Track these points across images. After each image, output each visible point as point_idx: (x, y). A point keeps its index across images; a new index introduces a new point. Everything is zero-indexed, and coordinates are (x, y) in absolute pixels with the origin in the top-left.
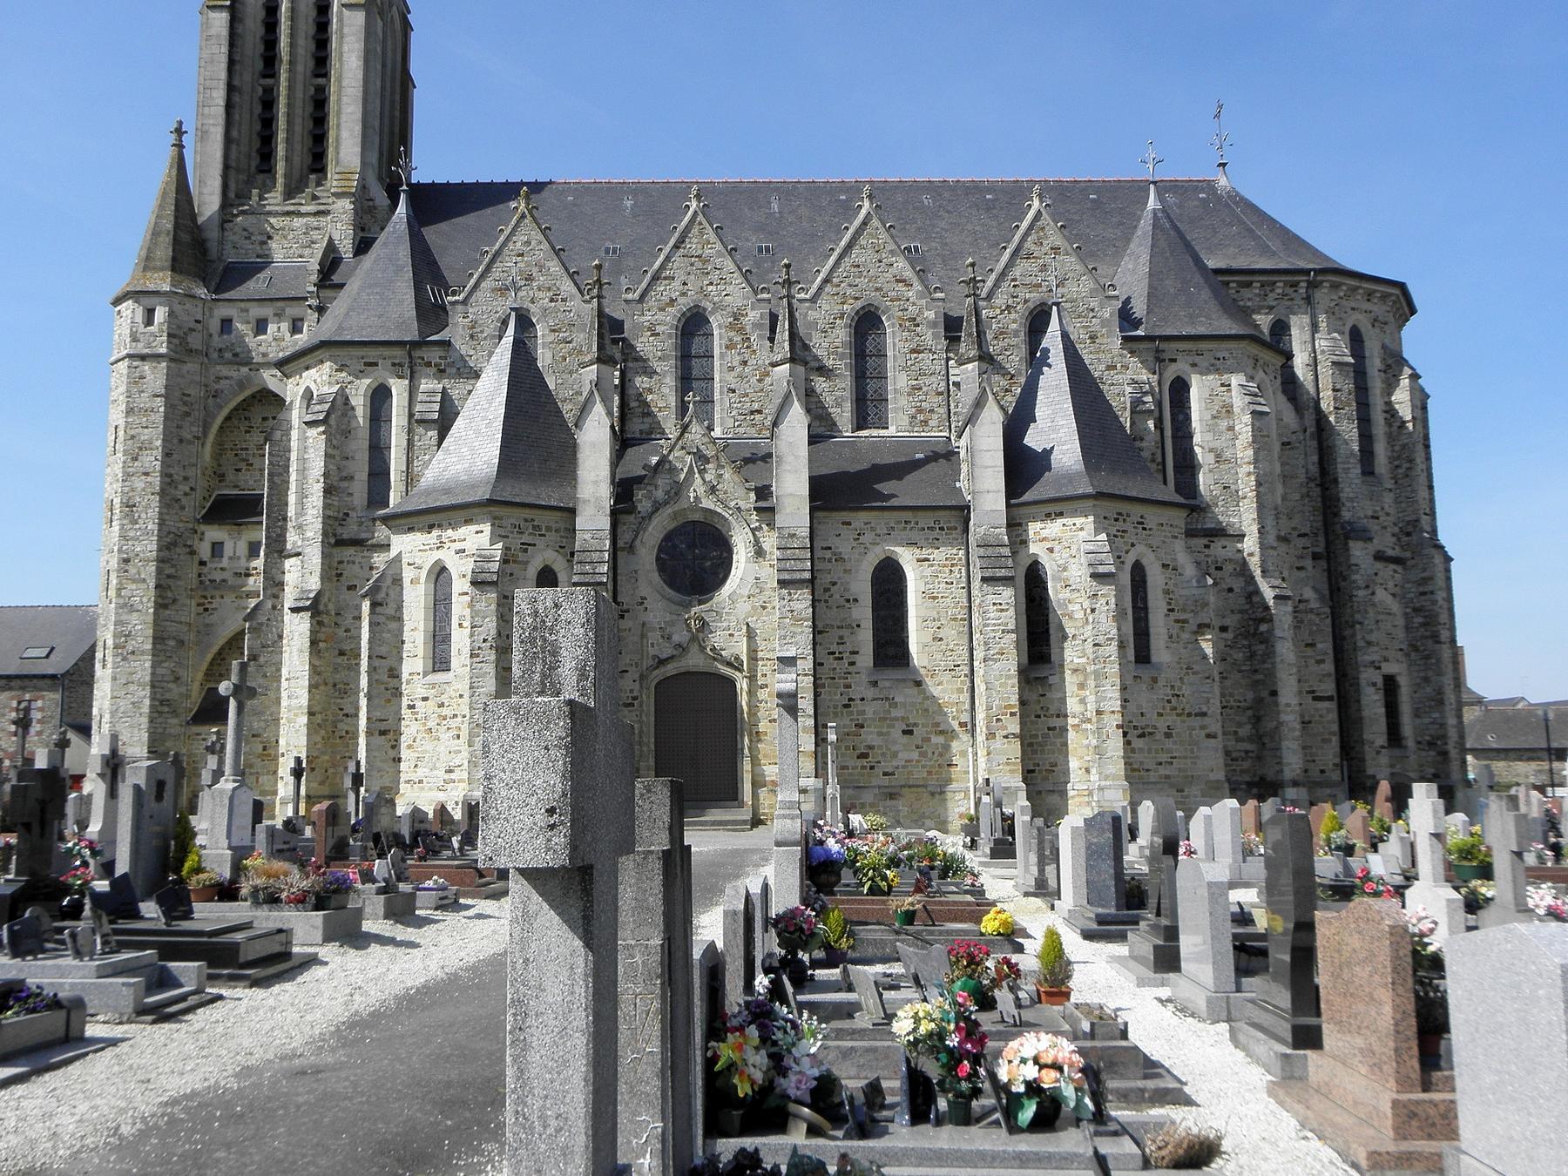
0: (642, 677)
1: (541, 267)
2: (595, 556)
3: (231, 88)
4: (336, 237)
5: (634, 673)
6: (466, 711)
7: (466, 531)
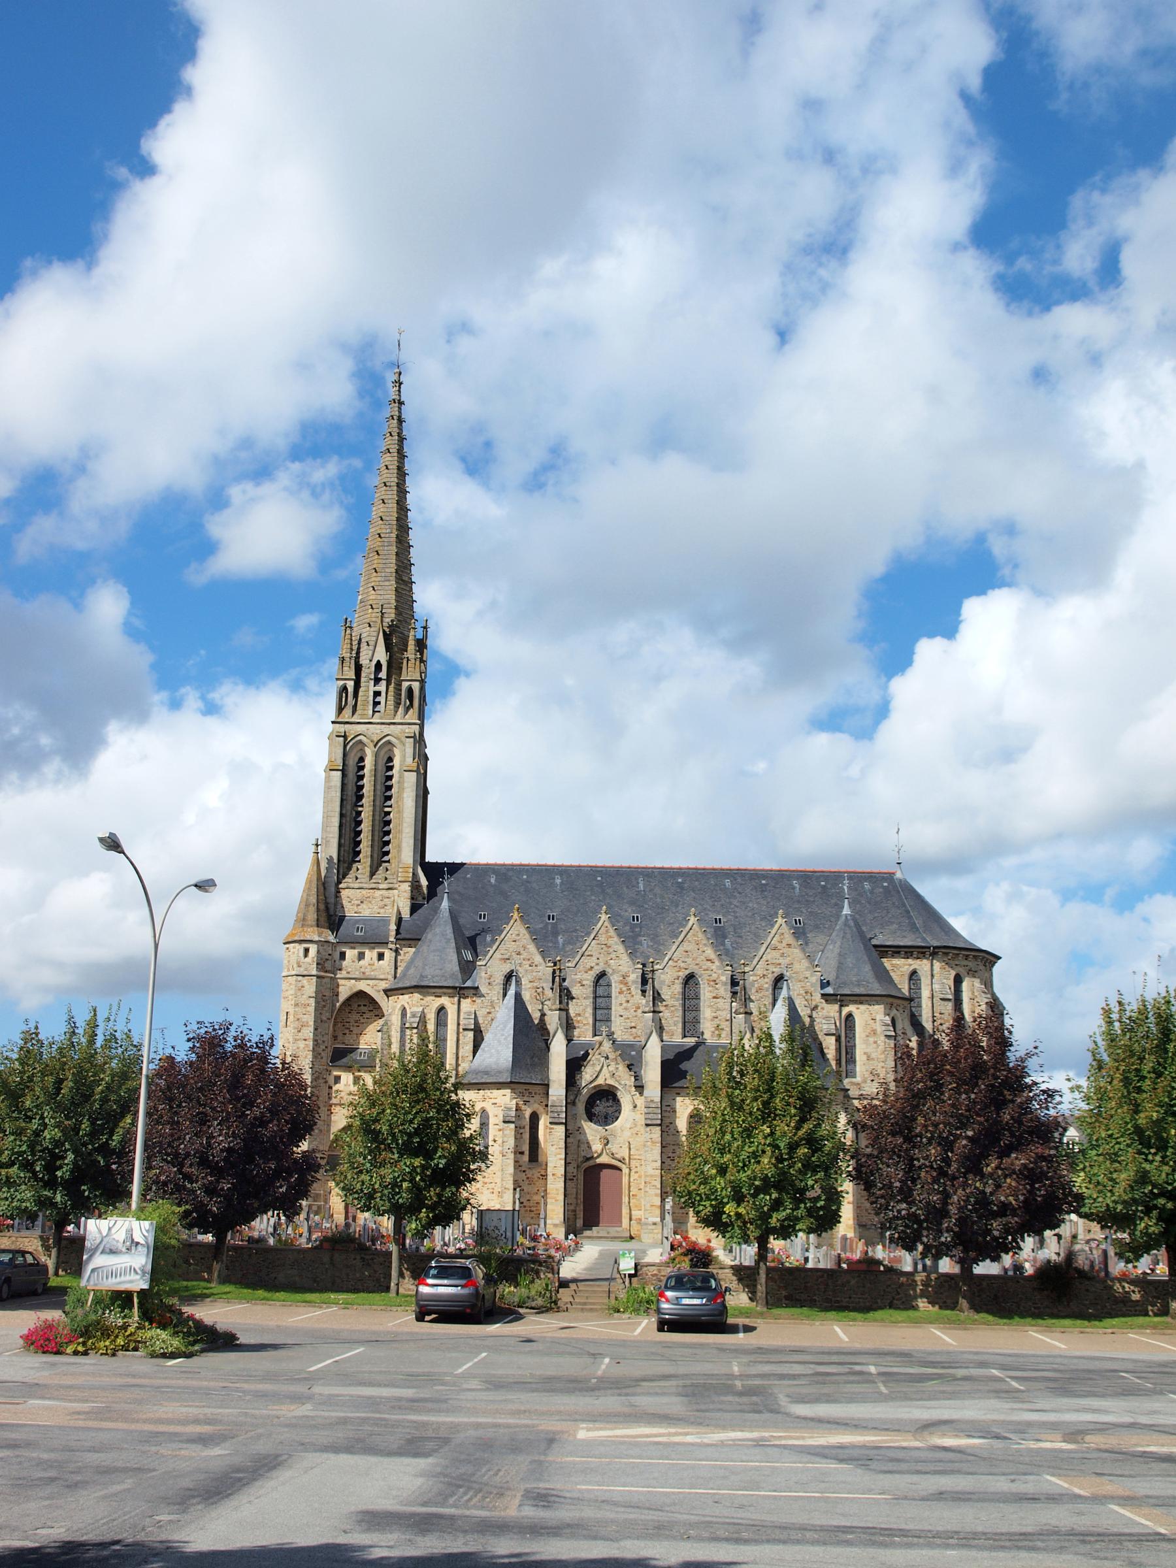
1: (525, 948)
2: (559, 1109)
3: (342, 815)
4: (401, 905)
5: (574, 1164)
6: (499, 1181)
7: (496, 1093)
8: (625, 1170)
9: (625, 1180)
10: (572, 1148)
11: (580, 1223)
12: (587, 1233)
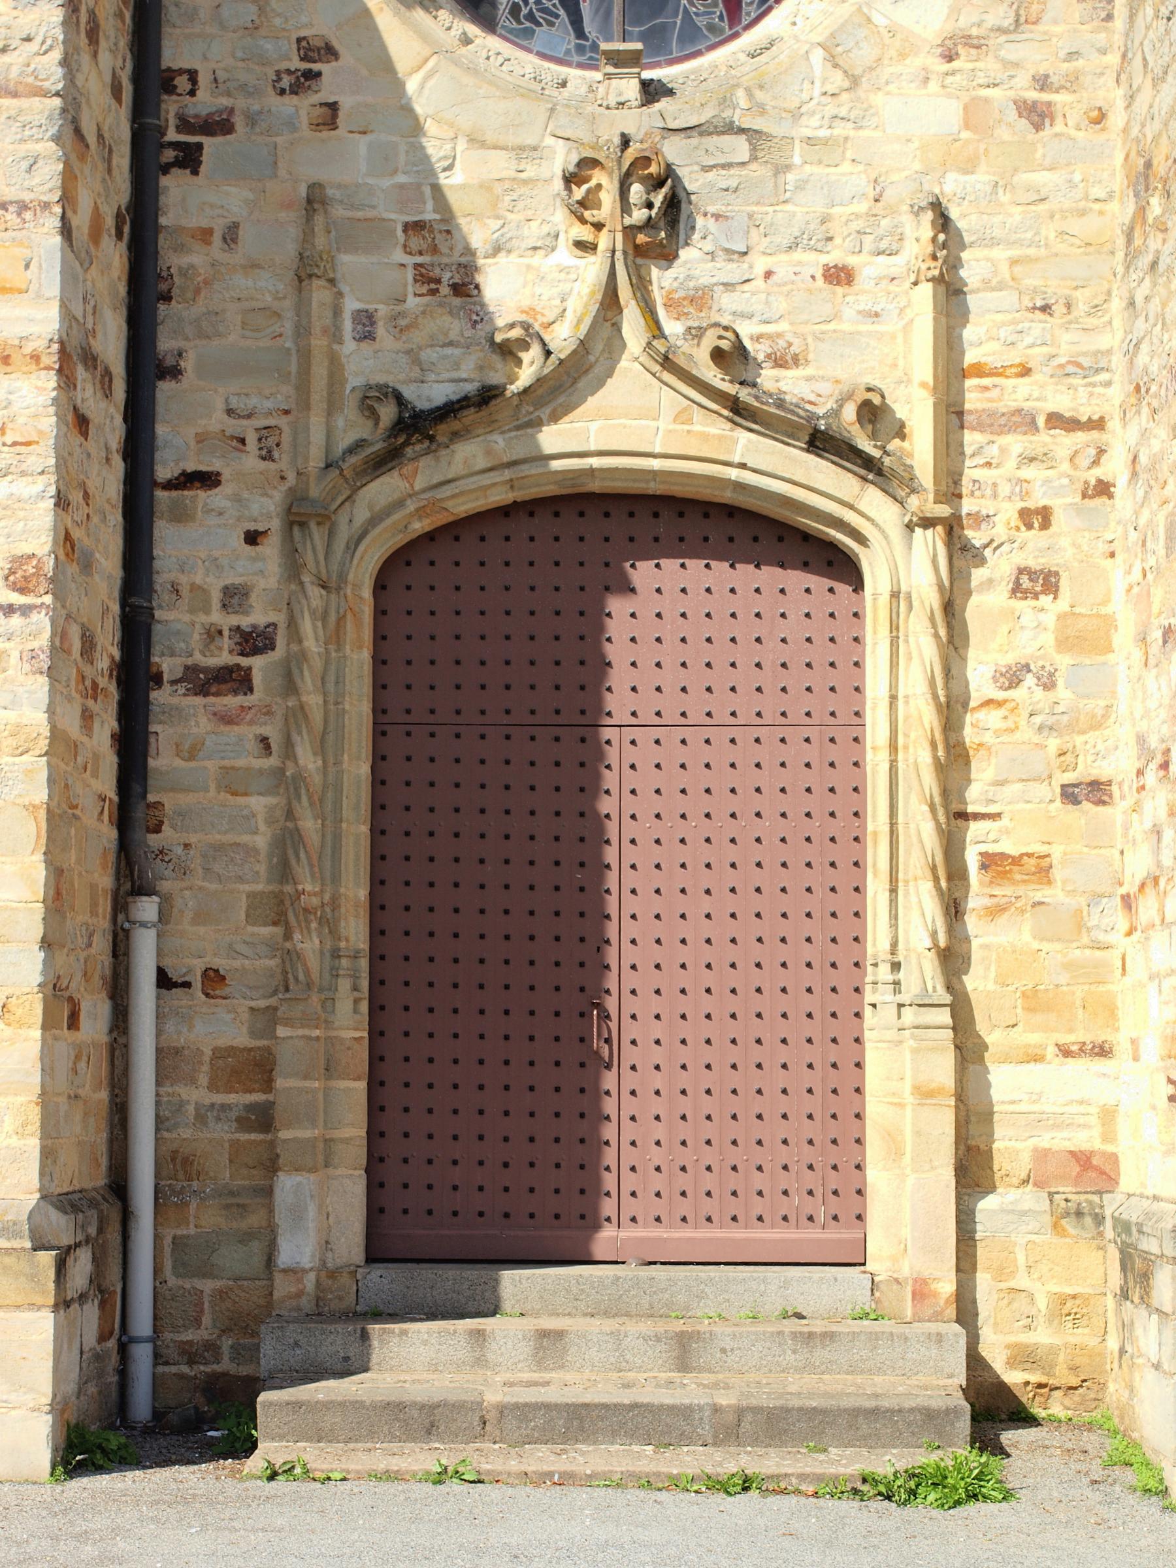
0: (299, 516)
5: (250, 495)
8: (898, 561)
9: (895, 681)
10: (227, 299)
11: (319, 1218)
12: (415, 1357)
